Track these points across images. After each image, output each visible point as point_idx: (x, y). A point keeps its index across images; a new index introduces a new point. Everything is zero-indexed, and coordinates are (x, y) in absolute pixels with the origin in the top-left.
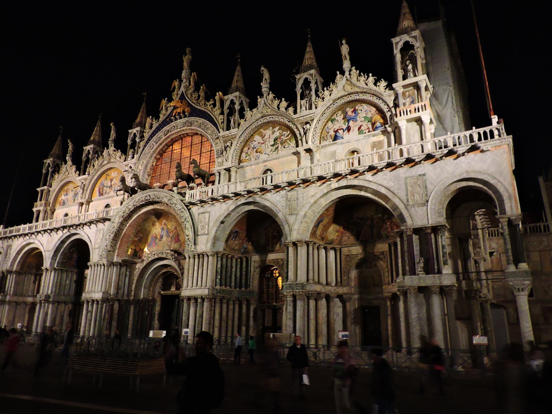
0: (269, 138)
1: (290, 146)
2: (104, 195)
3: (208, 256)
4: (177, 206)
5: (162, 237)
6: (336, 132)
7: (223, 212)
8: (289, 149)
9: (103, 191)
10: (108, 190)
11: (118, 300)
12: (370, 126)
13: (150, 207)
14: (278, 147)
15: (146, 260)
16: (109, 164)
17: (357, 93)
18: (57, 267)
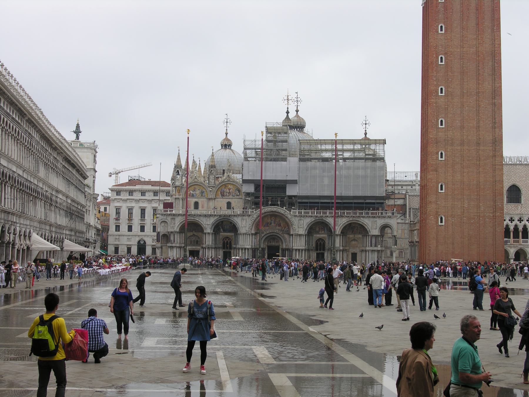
3: (303, 235)
5: (271, 223)
10: (228, 194)
11: (255, 249)
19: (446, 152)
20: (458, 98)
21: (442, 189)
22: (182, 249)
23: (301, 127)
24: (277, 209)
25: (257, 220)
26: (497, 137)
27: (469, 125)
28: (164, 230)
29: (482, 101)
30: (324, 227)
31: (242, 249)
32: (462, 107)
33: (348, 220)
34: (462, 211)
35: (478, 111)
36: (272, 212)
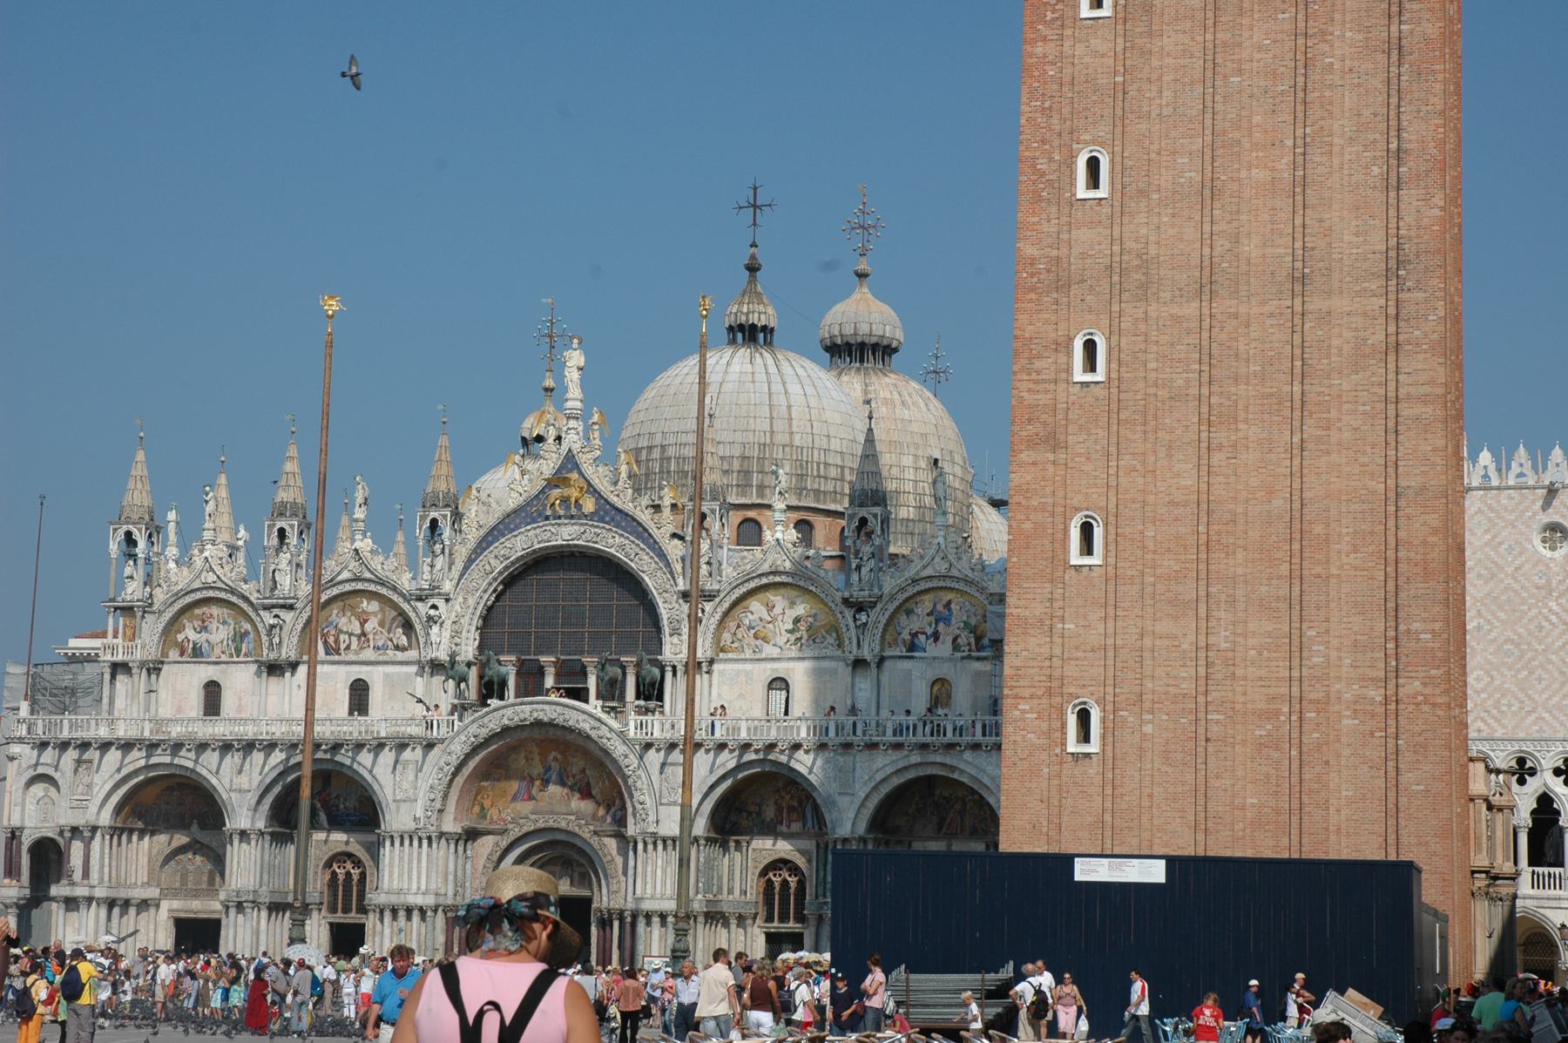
0: (784, 613)
2: (342, 651)
6: (914, 635)
9: (337, 641)
12: (973, 640)
14: (801, 638)
18: (266, 827)
19: (1115, 338)
20: (1188, 25)
21: (1087, 548)
22: (132, 911)
23: (875, 347)
25: (472, 764)
26: (1410, 239)
27: (1243, 174)
28: (46, 819)
29: (1323, 33)
30: (800, 802)
32: (1209, 74)
33: (900, 765)
34: (1202, 671)
35: (1301, 95)
36: (538, 724)
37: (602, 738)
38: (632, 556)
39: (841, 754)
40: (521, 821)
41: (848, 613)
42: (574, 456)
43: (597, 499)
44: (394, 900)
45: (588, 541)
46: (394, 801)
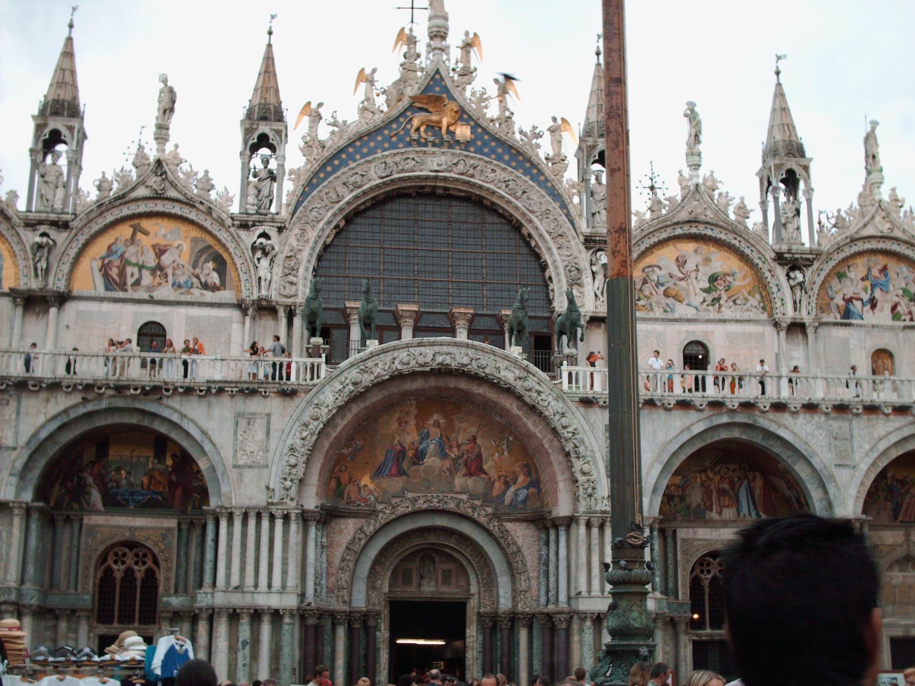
0: (697, 270)
1: (748, 305)
2: (129, 286)
4: (543, 396)
5: (420, 456)
6: (849, 301)
7: (672, 434)
8: (747, 310)
9: (122, 273)
10: (147, 279)
13: (432, 382)
14: (718, 299)
15: (387, 511)
16: (159, 202)
17: (896, 239)
18: (33, 501)
24: (471, 352)
25: (342, 424)
30: (732, 484)
31: (234, 616)
36: (444, 372)
37: (530, 390)
38: (519, 193)
39: (834, 419)
40: (394, 501)
41: (781, 272)
42: (442, 79)
43: (472, 128)
44: (236, 600)
45: (462, 174)
46: (235, 466)
